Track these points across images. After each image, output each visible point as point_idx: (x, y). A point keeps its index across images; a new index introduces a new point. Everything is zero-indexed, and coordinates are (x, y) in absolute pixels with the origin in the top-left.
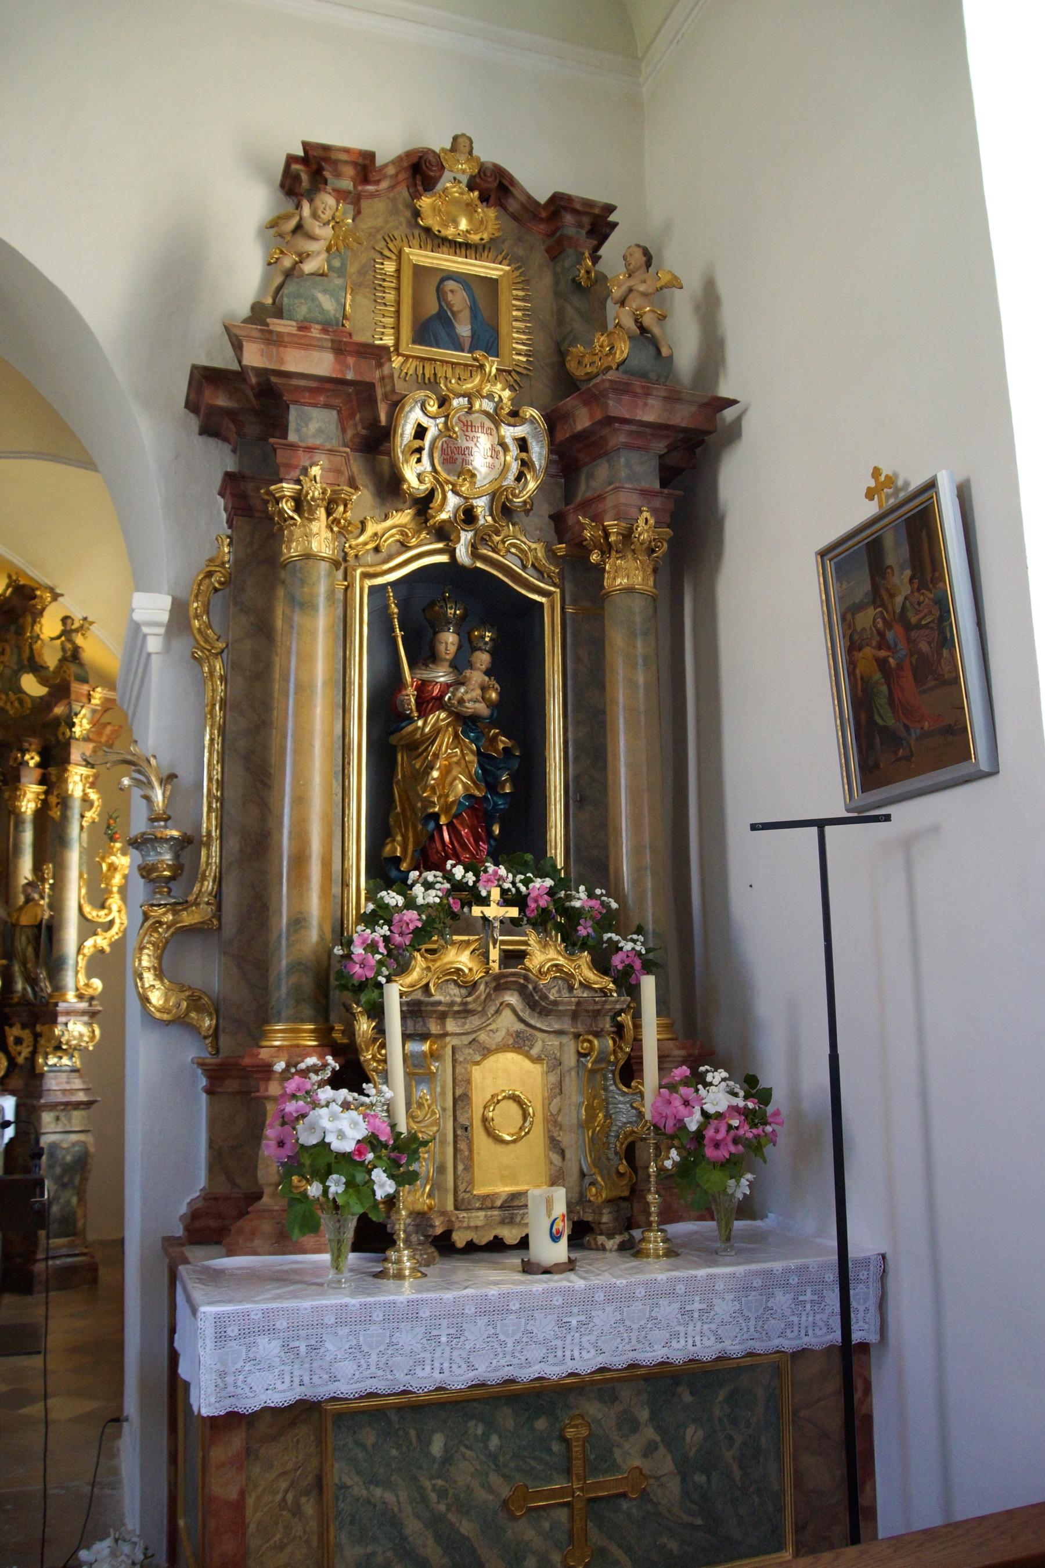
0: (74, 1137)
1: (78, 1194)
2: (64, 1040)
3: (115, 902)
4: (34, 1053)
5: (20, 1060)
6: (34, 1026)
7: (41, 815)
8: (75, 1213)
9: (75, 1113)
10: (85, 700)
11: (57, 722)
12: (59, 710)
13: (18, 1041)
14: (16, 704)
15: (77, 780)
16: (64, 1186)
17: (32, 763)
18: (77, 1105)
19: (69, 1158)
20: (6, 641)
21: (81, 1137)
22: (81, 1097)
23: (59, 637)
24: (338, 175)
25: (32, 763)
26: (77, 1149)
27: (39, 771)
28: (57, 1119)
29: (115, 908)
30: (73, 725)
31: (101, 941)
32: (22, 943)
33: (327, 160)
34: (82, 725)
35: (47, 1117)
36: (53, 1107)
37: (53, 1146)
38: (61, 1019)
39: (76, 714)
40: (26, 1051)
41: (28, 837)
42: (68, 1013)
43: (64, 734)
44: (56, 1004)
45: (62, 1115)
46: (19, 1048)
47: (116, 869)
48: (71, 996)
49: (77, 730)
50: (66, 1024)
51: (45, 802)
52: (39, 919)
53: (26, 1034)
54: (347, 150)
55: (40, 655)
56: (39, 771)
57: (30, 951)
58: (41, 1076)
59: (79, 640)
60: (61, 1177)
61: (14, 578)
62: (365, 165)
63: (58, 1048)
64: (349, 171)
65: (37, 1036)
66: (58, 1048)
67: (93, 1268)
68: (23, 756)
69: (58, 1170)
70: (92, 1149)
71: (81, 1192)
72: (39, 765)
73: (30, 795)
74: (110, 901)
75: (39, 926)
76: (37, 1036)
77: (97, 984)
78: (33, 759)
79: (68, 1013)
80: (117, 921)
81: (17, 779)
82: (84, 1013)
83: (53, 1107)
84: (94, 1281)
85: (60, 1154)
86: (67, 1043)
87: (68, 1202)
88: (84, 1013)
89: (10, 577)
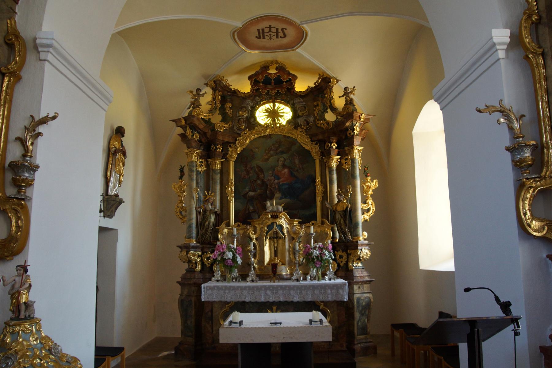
0: (365, 295)
1: (368, 318)
2: (361, 256)
3: (370, 201)
4: (347, 262)
5: (342, 264)
6: (346, 251)
7: (339, 167)
8: (367, 326)
9: (365, 285)
10: (358, 119)
11: (347, 129)
12: (348, 124)
13: (341, 257)
14: (326, 124)
15: (357, 151)
16: (362, 315)
17: (334, 147)
18: (366, 282)
19: (364, 303)
20: (318, 101)
21: (368, 295)
22: (367, 279)
23: (343, 96)
25: (334, 147)
26: (367, 300)
27: (337, 150)
28: (359, 288)
29: (370, 203)
30: (354, 129)
31: (367, 216)
32: (338, 217)
34: (357, 130)
35: (356, 287)
36: (357, 283)
37: (359, 299)
38: (359, 248)
39: (355, 126)
40: (344, 260)
41: (335, 176)
42: (362, 245)
43: (350, 134)
44: (357, 242)
45: (360, 286)
46: (341, 260)
47: (370, 188)
48: (361, 238)
49: (355, 131)
50: (361, 250)
51: (340, 162)
52: (345, 207)
53: (344, 254)
55: (334, 104)
56: (337, 150)
57: (342, 221)
58: (352, 271)
59: (352, 96)
60: (361, 311)
61: (321, 75)
63: (359, 259)
65: (348, 255)
66: (359, 259)
67: (375, 348)
68: (331, 145)
69: (360, 308)
70: (372, 300)
71: (368, 317)
72: (336, 148)
73: (335, 160)
74: (368, 200)
75: (345, 211)
76: (348, 255)
77: (366, 234)
78: (334, 146)
79: (362, 245)
80: (372, 208)
81: (330, 154)
82: (367, 245)
83: (357, 283)
84: (375, 353)
85: (361, 302)
86: (363, 257)
87: (364, 321)
88: (367, 245)
89: (319, 75)
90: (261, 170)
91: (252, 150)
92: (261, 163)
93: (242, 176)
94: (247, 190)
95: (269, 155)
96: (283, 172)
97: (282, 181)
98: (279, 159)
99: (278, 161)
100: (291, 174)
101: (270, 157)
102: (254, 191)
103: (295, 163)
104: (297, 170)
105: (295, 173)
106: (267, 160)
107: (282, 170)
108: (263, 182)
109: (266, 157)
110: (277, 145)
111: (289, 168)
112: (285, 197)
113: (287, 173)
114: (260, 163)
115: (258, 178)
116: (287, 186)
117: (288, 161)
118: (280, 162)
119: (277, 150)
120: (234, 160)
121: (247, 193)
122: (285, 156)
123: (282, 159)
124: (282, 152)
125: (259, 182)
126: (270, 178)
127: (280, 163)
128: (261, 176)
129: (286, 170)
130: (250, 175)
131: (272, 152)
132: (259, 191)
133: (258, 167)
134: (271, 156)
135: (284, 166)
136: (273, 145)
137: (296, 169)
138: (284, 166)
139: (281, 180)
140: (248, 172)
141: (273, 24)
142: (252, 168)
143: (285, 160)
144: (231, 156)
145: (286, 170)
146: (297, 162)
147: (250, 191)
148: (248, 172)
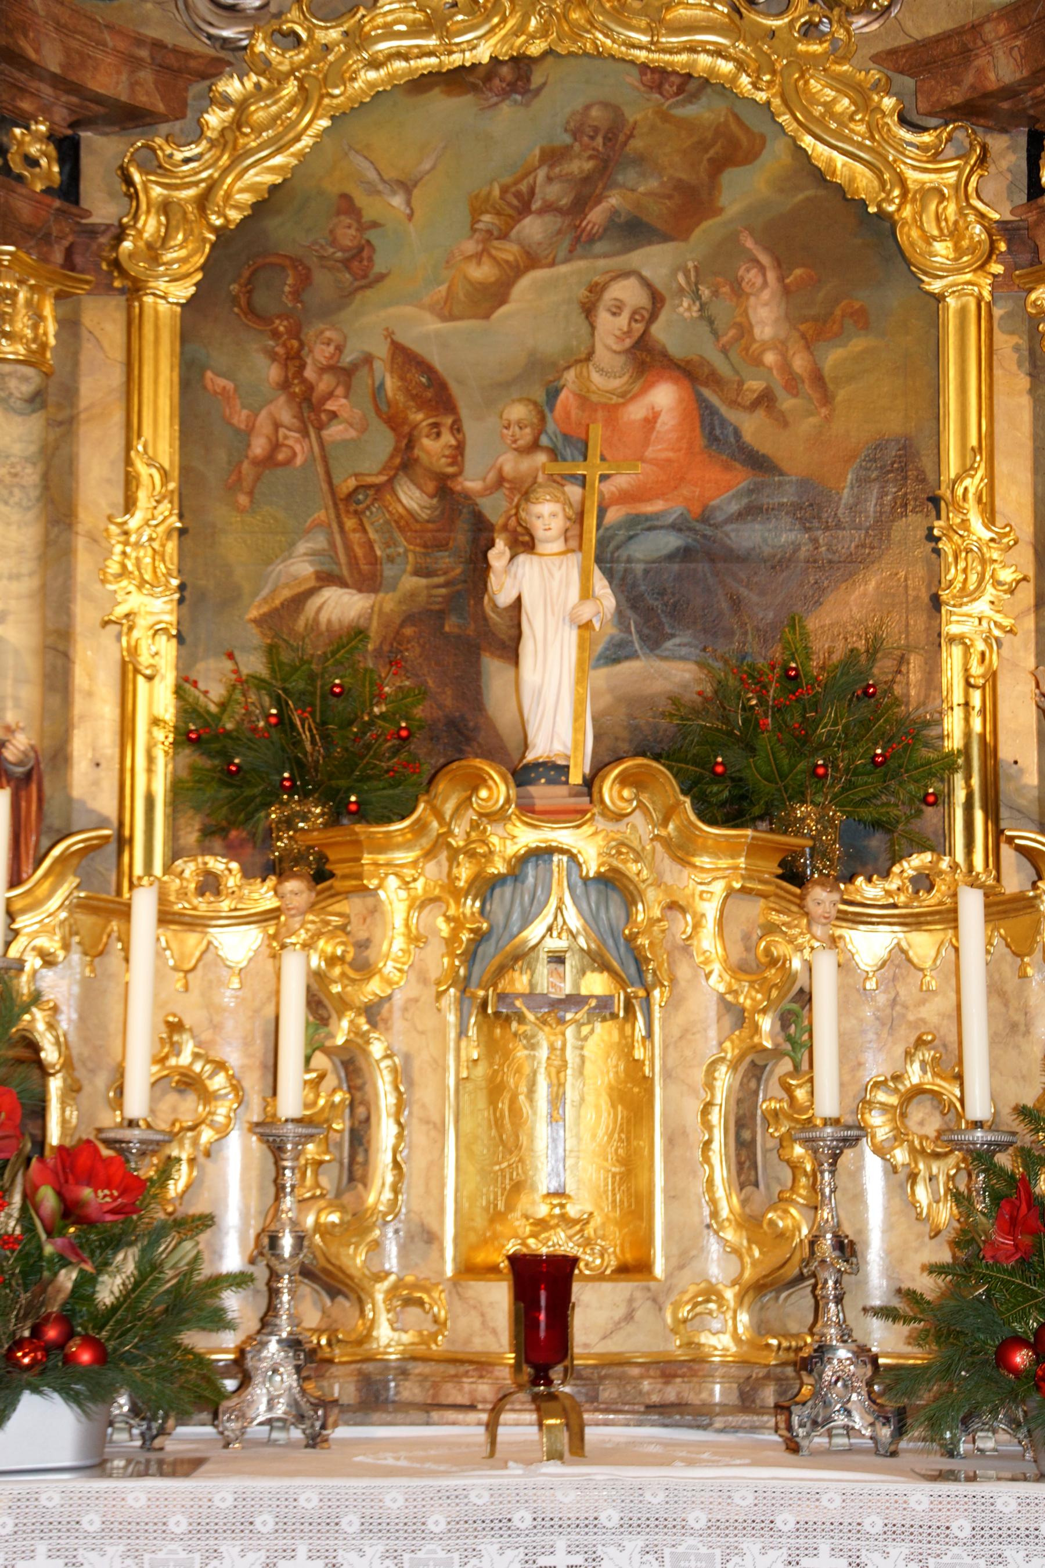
90: (437, 395)
91: (347, 206)
92: (434, 325)
93: (259, 447)
94: (301, 568)
95: (508, 251)
96: (636, 412)
97: (625, 497)
98: (596, 290)
99: (589, 310)
101: (514, 272)
102: (367, 580)
103: (745, 330)
104: (766, 400)
105: (752, 427)
106: (495, 295)
107: (628, 397)
108: (444, 489)
109: (482, 272)
110: (579, 166)
111: (689, 373)
112: (654, 640)
113: (667, 422)
114: (425, 331)
115: (405, 461)
116: (672, 541)
117: (686, 308)
118: (603, 318)
119: (580, 205)
120: (183, 291)
121: (299, 600)
122: (656, 261)
123: (627, 292)
124: (634, 230)
125: (411, 497)
126: (510, 464)
127: (611, 327)
128: (433, 448)
130: (335, 432)
131: (533, 228)
132: (410, 582)
133: (405, 358)
134: (531, 261)
135: (646, 358)
136: (552, 156)
137: (755, 385)
138: (646, 358)
140: (311, 410)
142: (346, 374)
143: (657, 299)
144: (153, 252)
145: (664, 396)
146: (765, 317)
147: (327, 578)
148: (311, 410)
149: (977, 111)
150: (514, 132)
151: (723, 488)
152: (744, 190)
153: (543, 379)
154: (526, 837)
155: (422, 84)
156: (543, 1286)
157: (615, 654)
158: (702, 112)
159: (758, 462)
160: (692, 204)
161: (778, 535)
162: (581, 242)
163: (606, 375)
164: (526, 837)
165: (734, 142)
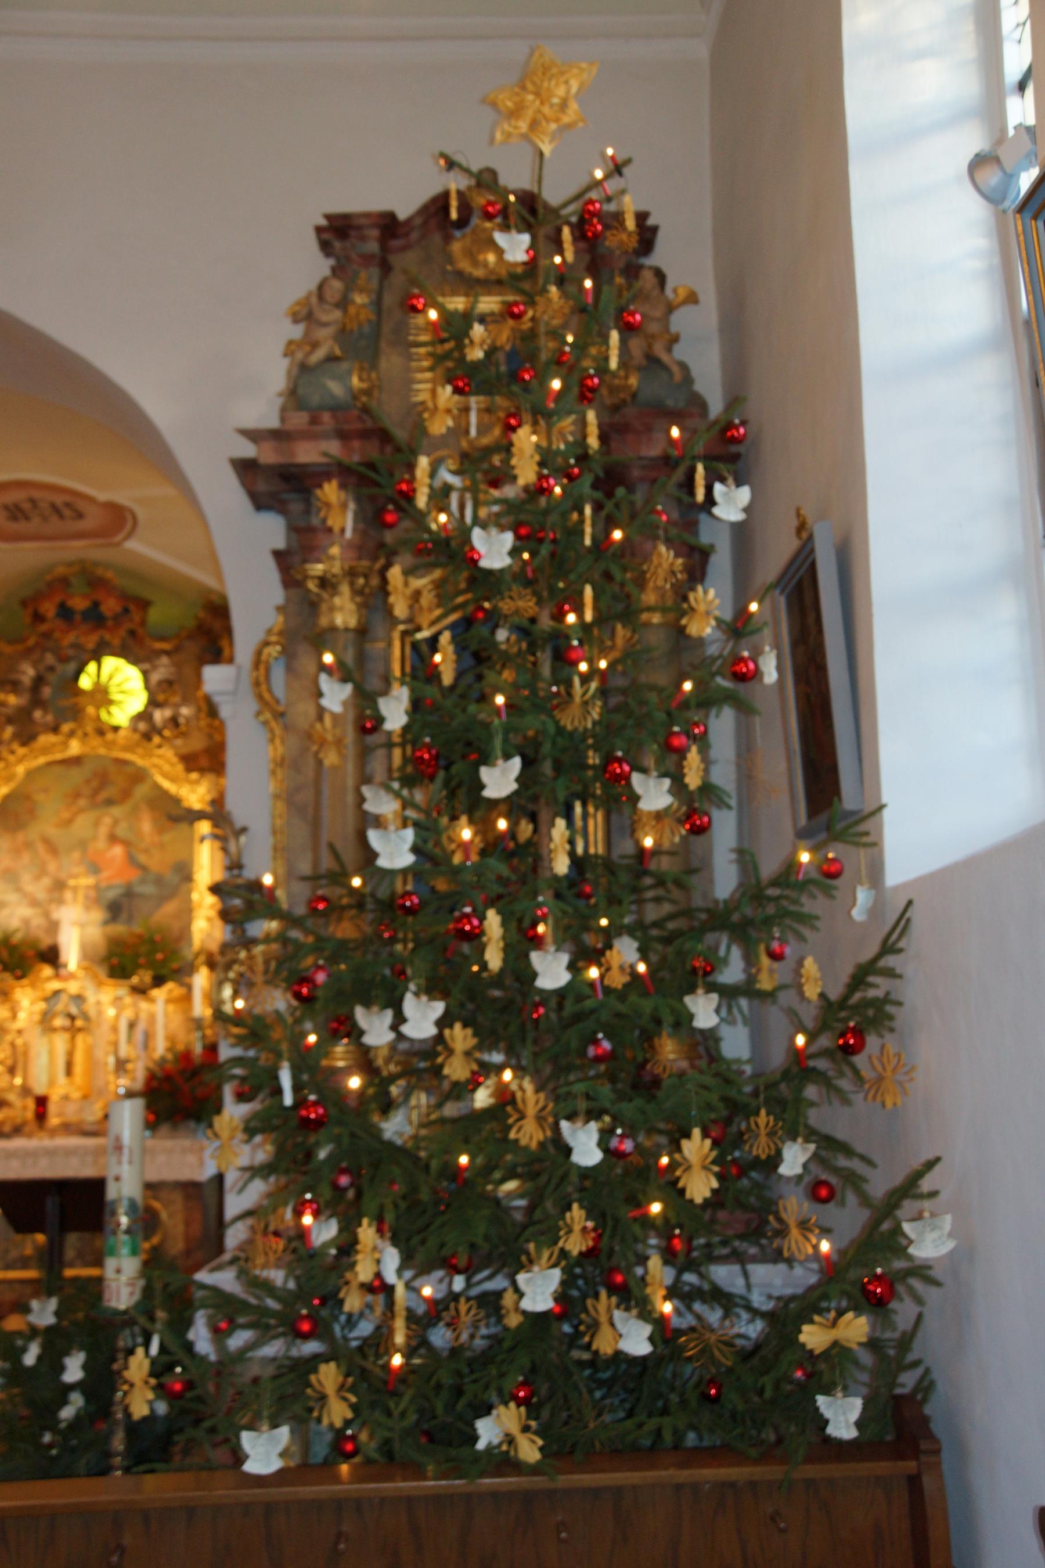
24: (363, 239)
33: (350, 227)
54: (367, 215)
62: (388, 225)
64: (375, 233)
100: (131, 860)
105: (142, 858)
106: (69, 822)
111: (126, 843)
122: (116, 811)
123: (107, 820)
124: (110, 802)
127: (103, 831)
129: (118, 851)
134: (82, 810)
136: (88, 781)
138: (113, 839)
139: (105, 874)
141: (37, 494)
145: (118, 851)
149: (202, 771)
150: (77, 775)
151: (134, 875)
152: (141, 791)
153: (83, 844)
154: (56, 985)
155: (49, 764)
156: (42, 1102)
157: (106, 923)
158: (129, 769)
159: (143, 868)
160: (126, 795)
161: (148, 889)
162: (94, 805)
163: (101, 844)
164: (56, 985)
165: (139, 776)
